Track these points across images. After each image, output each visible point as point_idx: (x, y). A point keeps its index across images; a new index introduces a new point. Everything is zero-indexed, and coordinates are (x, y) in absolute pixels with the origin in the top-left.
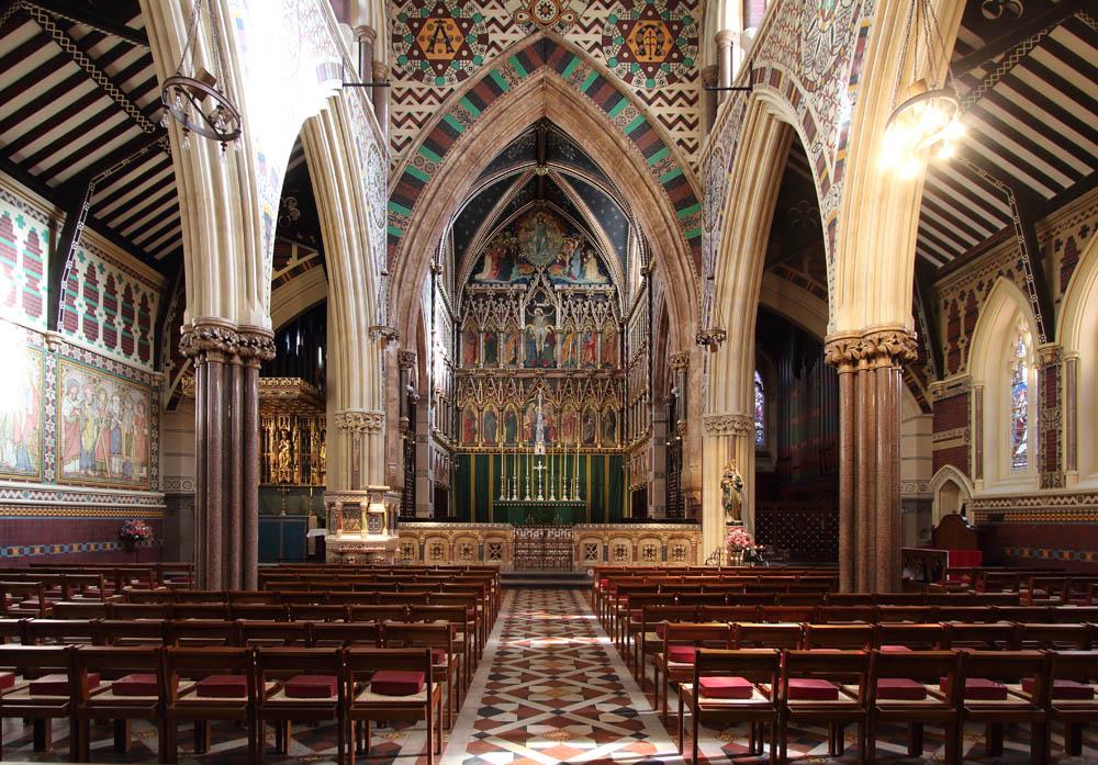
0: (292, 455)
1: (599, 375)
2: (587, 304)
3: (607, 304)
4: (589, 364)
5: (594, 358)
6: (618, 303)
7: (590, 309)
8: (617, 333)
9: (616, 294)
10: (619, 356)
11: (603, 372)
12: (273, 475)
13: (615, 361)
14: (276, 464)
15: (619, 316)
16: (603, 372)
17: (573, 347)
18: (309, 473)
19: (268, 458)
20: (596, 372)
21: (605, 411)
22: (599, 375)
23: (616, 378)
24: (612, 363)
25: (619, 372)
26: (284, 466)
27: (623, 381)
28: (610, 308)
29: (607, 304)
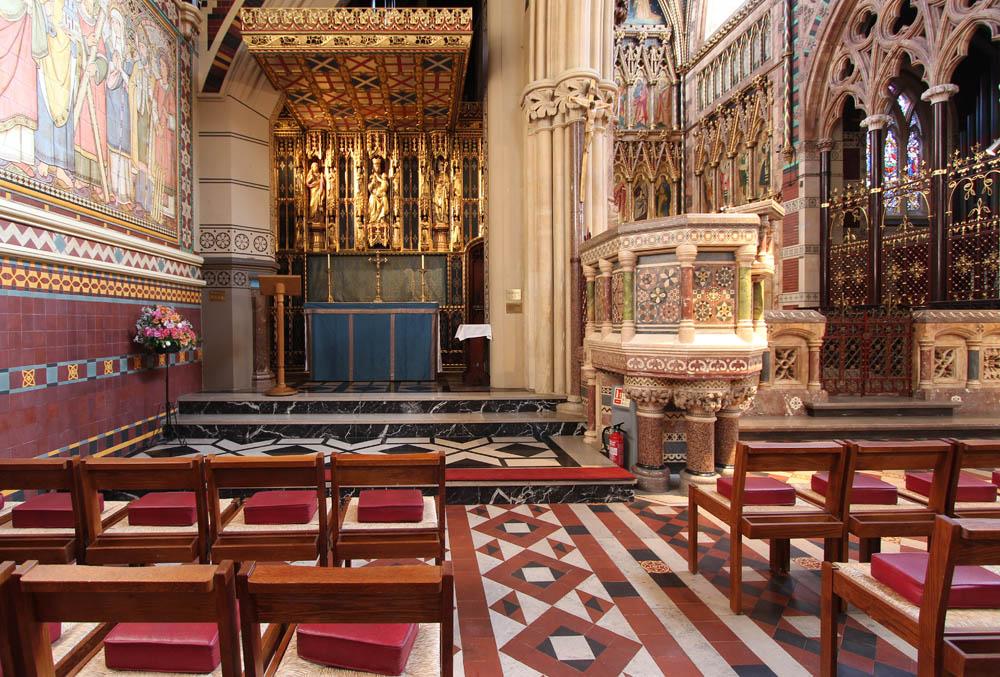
0: (390, 202)
1: (653, 138)
2: (638, 49)
3: (661, 49)
4: (639, 124)
5: (646, 117)
6: (672, 50)
7: (641, 57)
8: (672, 85)
9: (673, 38)
10: (675, 114)
11: (658, 134)
12: (359, 234)
13: (670, 120)
14: (364, 217)
15: (674, 64)
16: (658, 134)
17: (622, 103)
18: (416, 232)
19: (350, 206)
20: (650, 133)
21: (660, 180)
22: (653, 138)
23: (674, 142)
24: (665, 123)
25: (674, 133)
26: (377, 216)
27: (680, 145)
28: (664, 56)
29: (661, 49)
